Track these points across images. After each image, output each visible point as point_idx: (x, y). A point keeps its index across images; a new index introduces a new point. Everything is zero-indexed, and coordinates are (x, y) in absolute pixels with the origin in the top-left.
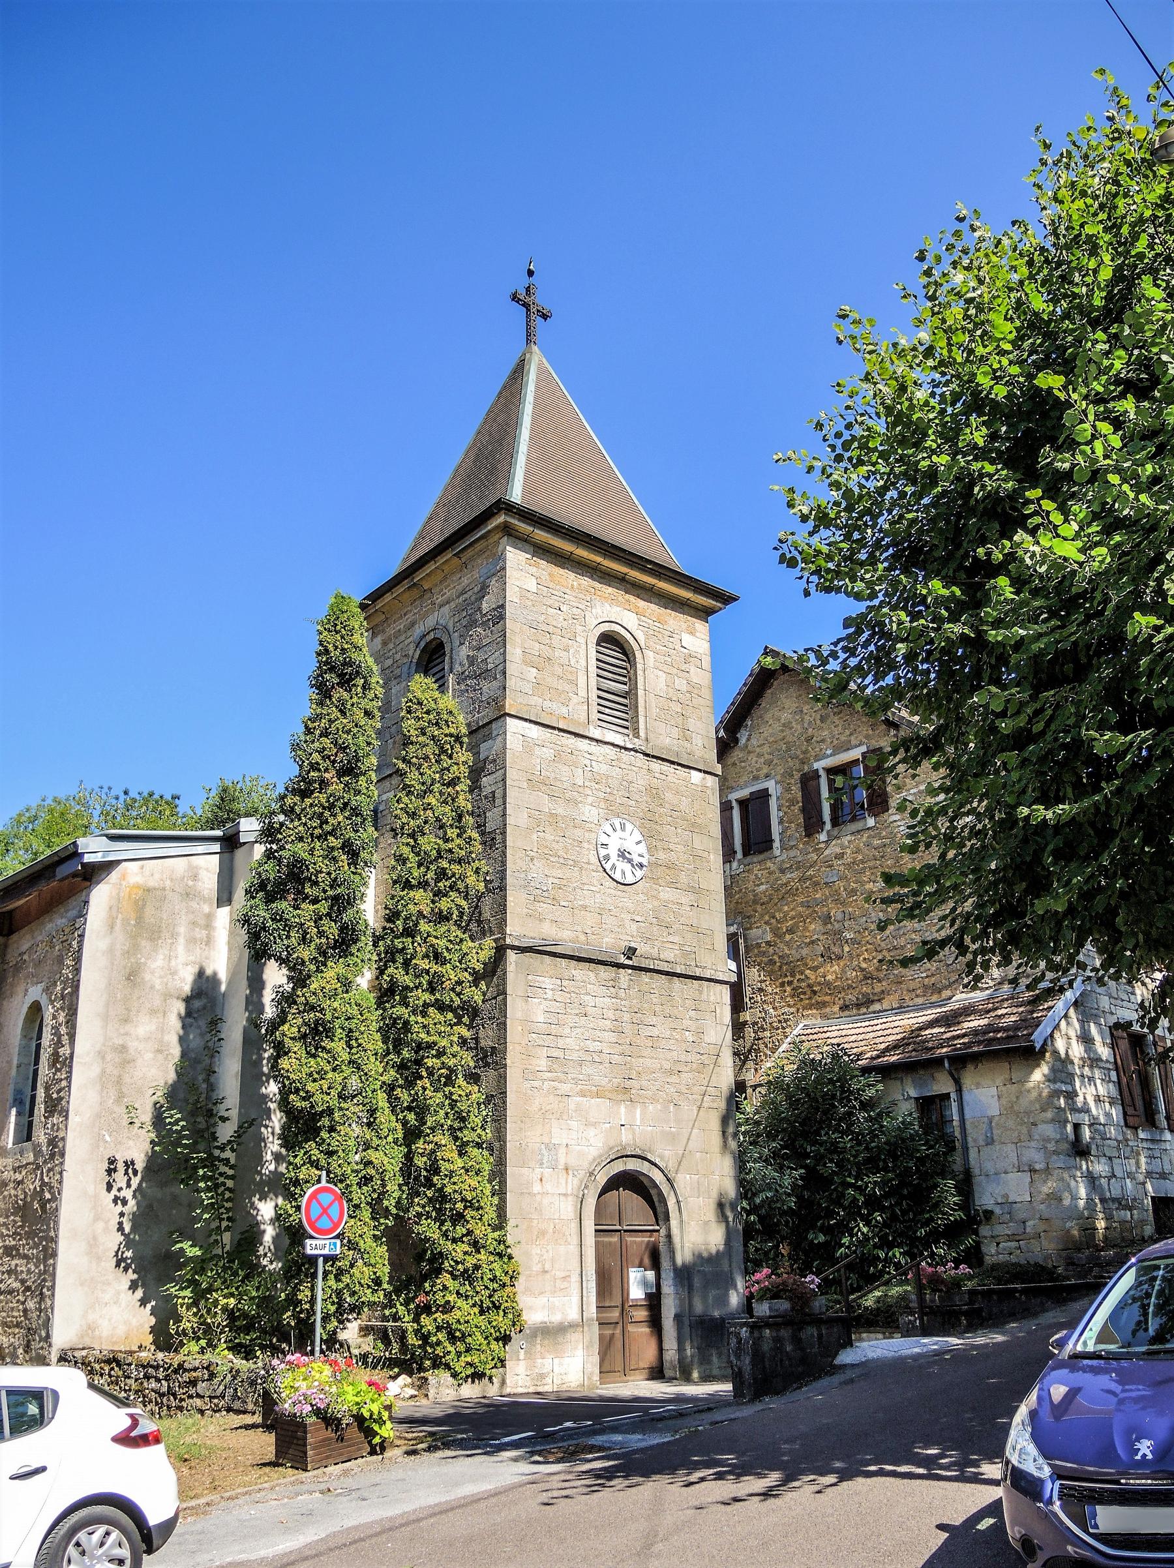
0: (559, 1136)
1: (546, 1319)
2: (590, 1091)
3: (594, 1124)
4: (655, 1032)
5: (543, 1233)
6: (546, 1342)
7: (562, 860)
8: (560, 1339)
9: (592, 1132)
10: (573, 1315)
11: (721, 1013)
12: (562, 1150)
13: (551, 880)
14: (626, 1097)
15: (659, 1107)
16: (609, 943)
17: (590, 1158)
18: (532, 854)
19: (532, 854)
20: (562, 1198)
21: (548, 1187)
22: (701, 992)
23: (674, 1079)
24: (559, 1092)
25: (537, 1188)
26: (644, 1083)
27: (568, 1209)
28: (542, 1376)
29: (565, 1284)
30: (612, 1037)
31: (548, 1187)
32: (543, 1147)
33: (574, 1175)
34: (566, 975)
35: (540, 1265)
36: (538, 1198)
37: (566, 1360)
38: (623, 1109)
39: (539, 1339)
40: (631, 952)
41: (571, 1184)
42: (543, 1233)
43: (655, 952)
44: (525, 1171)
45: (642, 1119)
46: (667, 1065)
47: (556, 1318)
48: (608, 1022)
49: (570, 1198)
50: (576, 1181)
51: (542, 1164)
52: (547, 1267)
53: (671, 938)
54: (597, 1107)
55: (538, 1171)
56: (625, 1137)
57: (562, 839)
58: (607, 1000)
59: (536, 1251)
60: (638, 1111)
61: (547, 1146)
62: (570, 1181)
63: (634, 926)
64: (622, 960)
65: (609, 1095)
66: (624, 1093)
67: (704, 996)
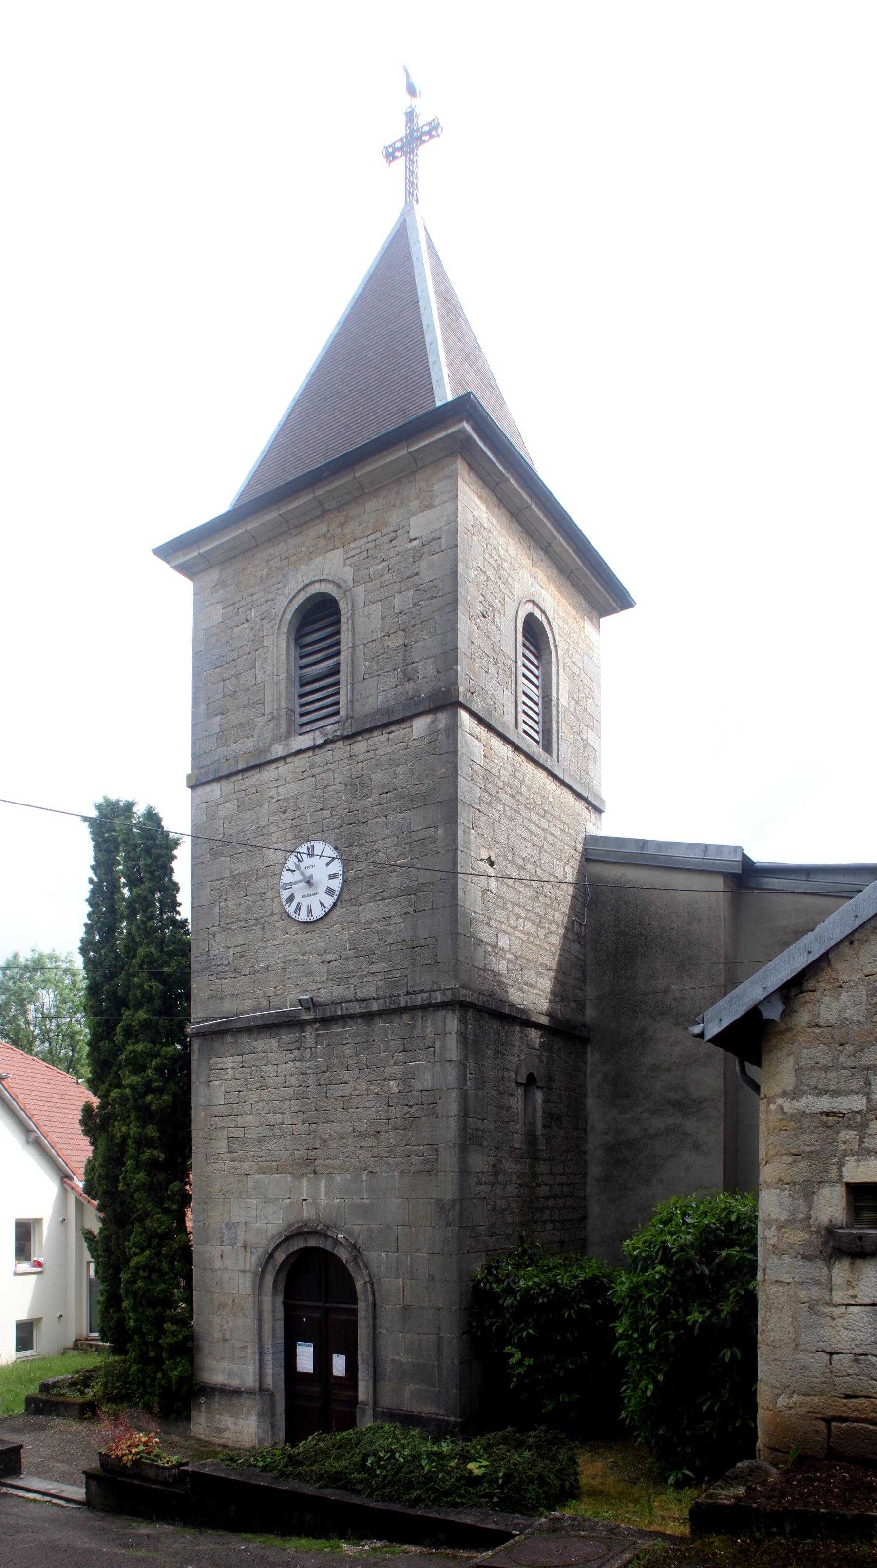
0: (238, 1215)
1: (226, 1382)
2: (271, 1167)
3: (274, 1201)
4: (347, 1089)
5: (222, 1306)
6: (223, 1402)
7: (243, 924)
8: (236, 1402)
9: (271, 1209)
10: (250, 1381)
11: (443, 1047)
12: (241, 1230)
13: (231, 951)
14: (311, 1169)
15: (348, 1176)
16: (289, 1001)
17: (269, 1235)
18: (214, 929)
19: (214, 929)
20: (241, 1274)
21: (228, 1263)
22: (413, 1027)
23: (371, 1141)
24: (239, 1172)
25: (218, 1264)
26: (332, 1151)
27: (244, 1284)
28: (220, 1431)
29: (243, 1354)
30: (295, 1105)
31: (228, 1263)
32: (223, 1226)
33: (252, 1253)
34: (247, 1049)
35: (220, 1334)
36: (219, 1273)
37: (241, 1422)
38: (305, 1183)
39: (217, 1399)
40: (312, 1004)
41: (251, 1261)
42: (222, 1306)
43: (350, 994)
44: (208, 1248)
45: (327, 1193)
46: (362, 1127)
47: (235, 1383)
48: (290, 1091)
49: (248, 1275)
50: (254, 1259)
51: (222, 1242)
52: (227, 1336)
53: (374, 968)
54: (278, 1182)
55: (219, 1247)
56: (307, 1213)
57: (243, 901)
58: (291, 1064)
59: (217, 1320)
60: (323, 1184)
61: (227, 1224)
62: (248, 1257)
63: (324, 968)
64: (305, 1016)
65: (290, 1169)
66: (308, 1166)
67: (418, 1031)
